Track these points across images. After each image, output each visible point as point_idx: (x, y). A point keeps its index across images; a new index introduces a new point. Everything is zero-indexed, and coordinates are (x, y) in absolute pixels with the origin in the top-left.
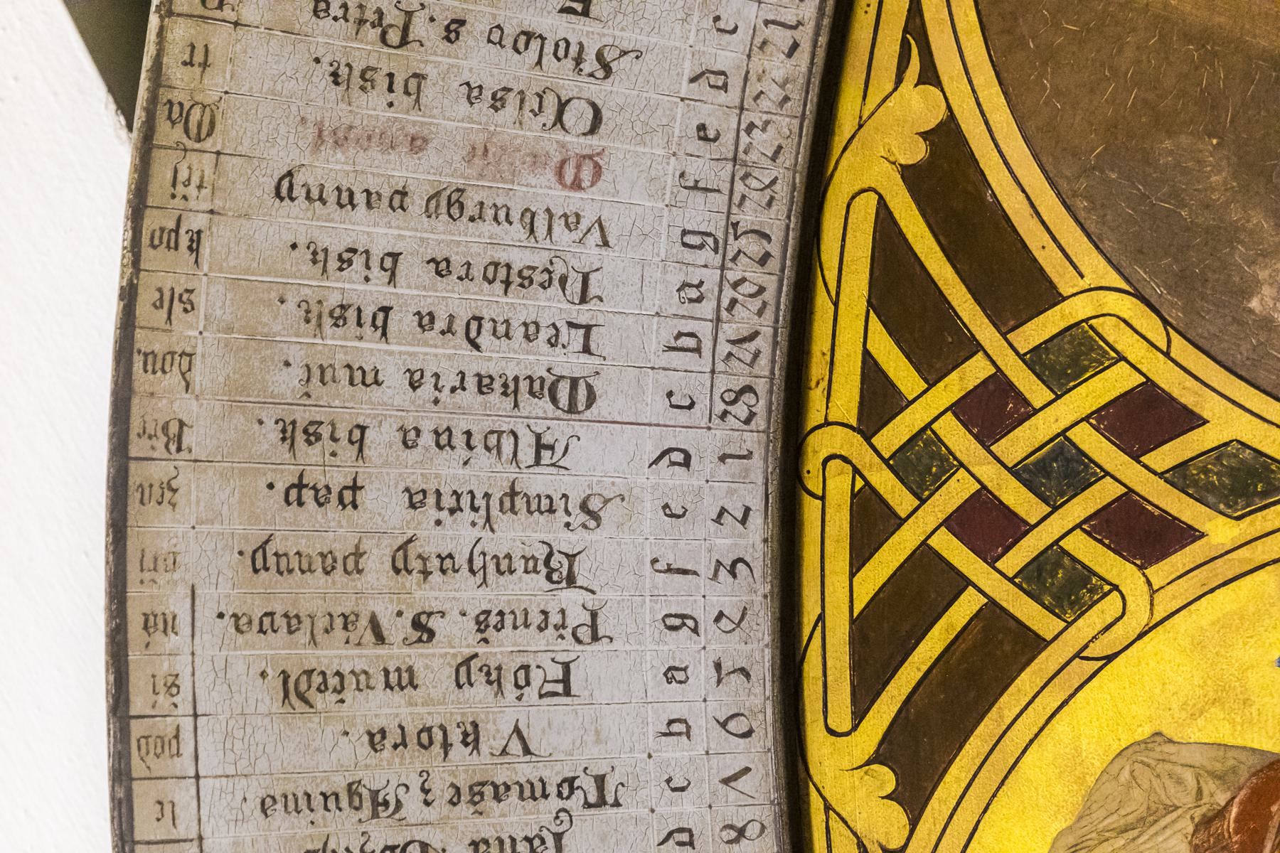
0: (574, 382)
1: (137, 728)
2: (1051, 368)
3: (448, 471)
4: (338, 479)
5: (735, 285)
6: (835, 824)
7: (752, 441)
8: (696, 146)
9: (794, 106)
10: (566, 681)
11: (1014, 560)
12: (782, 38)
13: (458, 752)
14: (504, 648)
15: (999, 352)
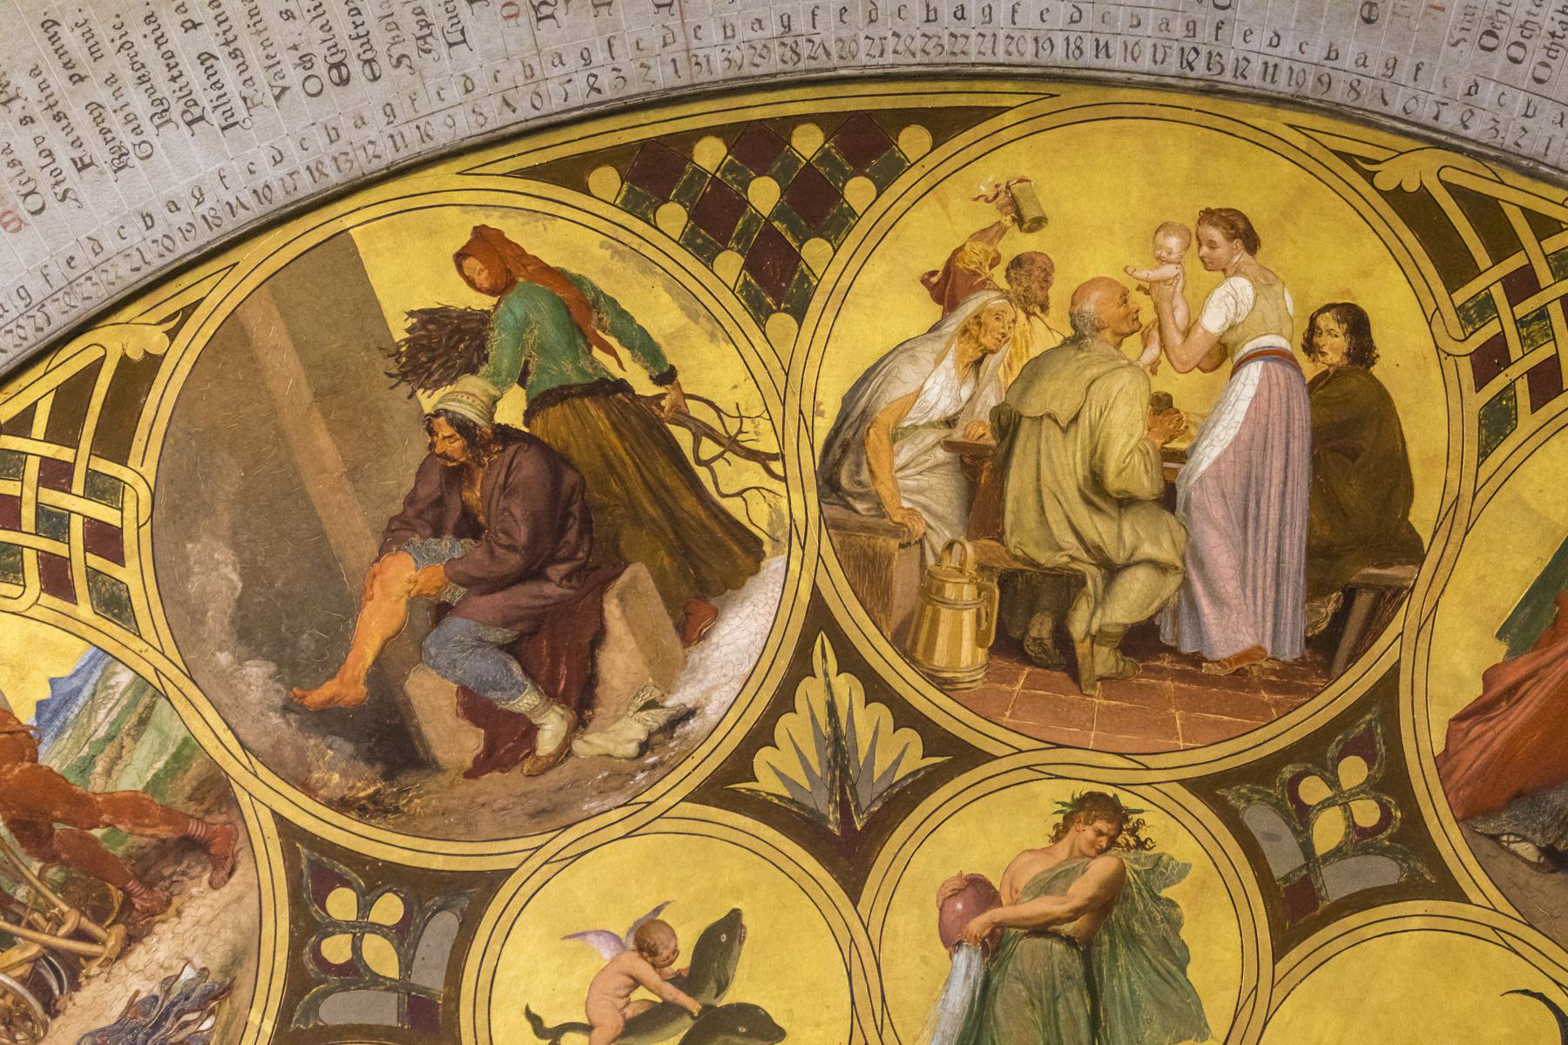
2: (93, 485)
5: (19, 326)
9: (113, 289)
12: (136, 260)
15: (82, 457)
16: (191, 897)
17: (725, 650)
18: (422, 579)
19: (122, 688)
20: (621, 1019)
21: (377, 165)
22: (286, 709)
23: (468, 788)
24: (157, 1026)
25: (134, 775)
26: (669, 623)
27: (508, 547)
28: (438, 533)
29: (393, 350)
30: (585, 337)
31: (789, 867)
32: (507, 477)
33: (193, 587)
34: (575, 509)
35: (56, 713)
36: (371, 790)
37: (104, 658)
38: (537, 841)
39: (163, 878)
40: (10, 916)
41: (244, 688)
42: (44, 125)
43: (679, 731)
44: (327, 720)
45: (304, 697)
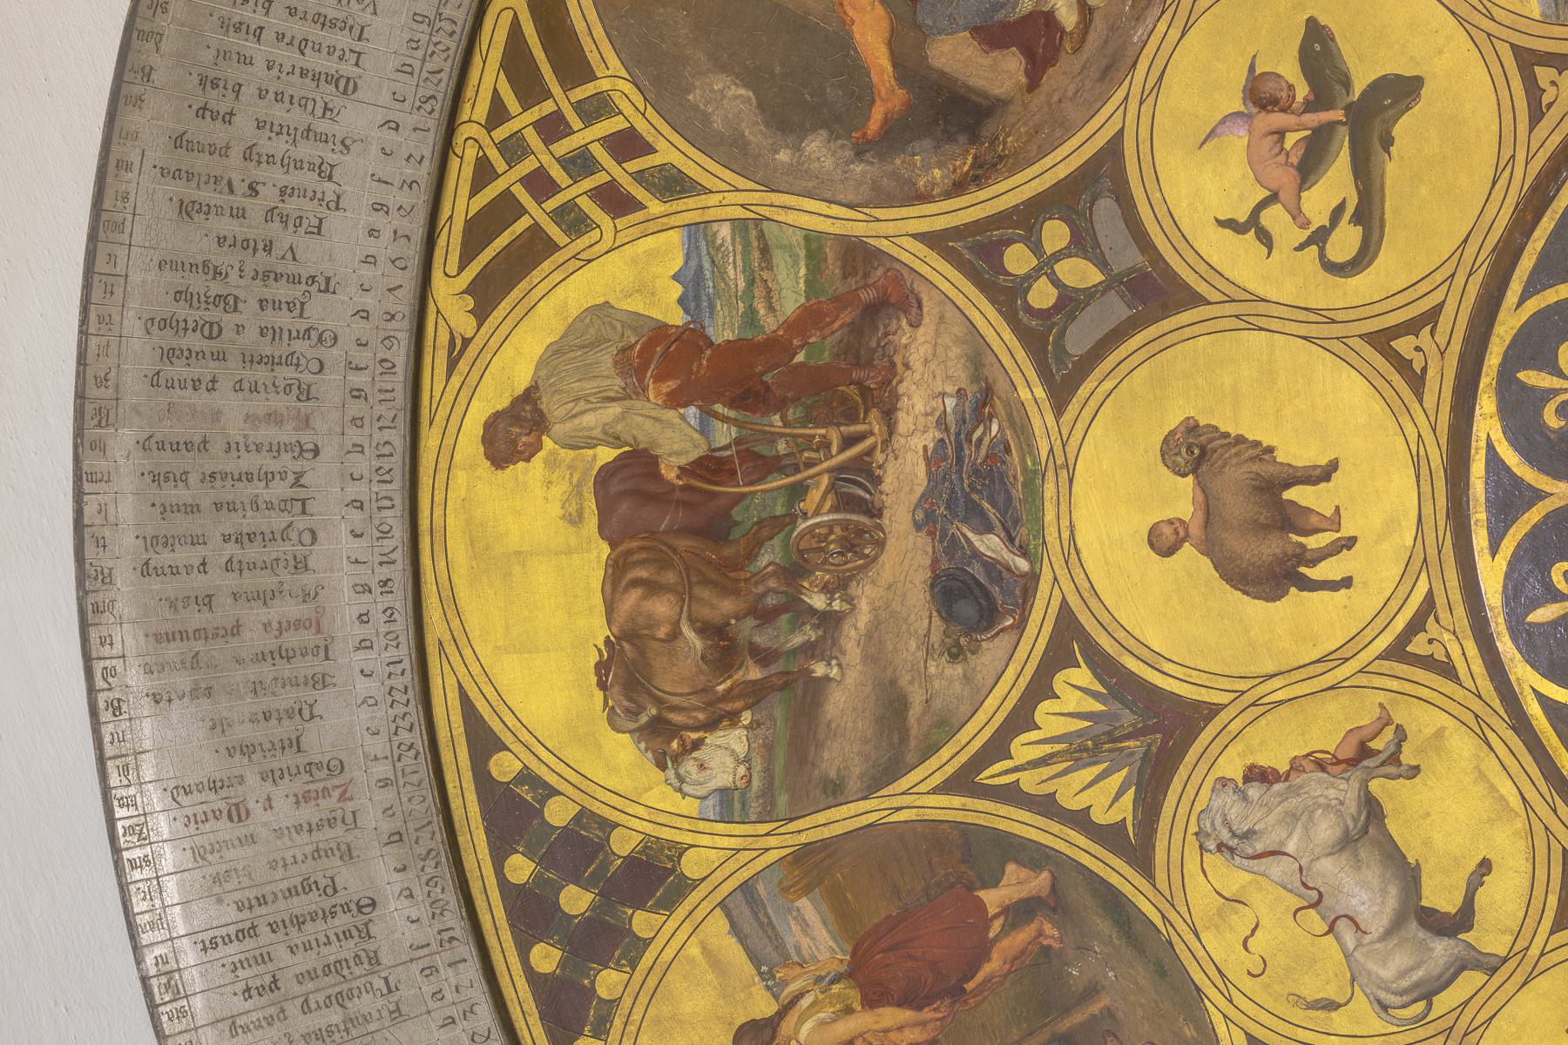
0: (348, 80)
3: (279, 113)
4: (224, 108)
6: (441, 321)
7: (431, 123)
10: (319, 228)
11: (551, 204)
13: (261, 253)
14: (291, 206)
15: (561, 100)
19: (729, 240)
22: (859, 155)
23: (1039, 98)
24: (960, 460)
25: (791, 294)
33: (718, 124)
35: (697, 298)
37: (697, 232)
38: (1121, 94)
39: (874, 351)
40: (788, 471)
41: (816, 165)
44: (895, 137)
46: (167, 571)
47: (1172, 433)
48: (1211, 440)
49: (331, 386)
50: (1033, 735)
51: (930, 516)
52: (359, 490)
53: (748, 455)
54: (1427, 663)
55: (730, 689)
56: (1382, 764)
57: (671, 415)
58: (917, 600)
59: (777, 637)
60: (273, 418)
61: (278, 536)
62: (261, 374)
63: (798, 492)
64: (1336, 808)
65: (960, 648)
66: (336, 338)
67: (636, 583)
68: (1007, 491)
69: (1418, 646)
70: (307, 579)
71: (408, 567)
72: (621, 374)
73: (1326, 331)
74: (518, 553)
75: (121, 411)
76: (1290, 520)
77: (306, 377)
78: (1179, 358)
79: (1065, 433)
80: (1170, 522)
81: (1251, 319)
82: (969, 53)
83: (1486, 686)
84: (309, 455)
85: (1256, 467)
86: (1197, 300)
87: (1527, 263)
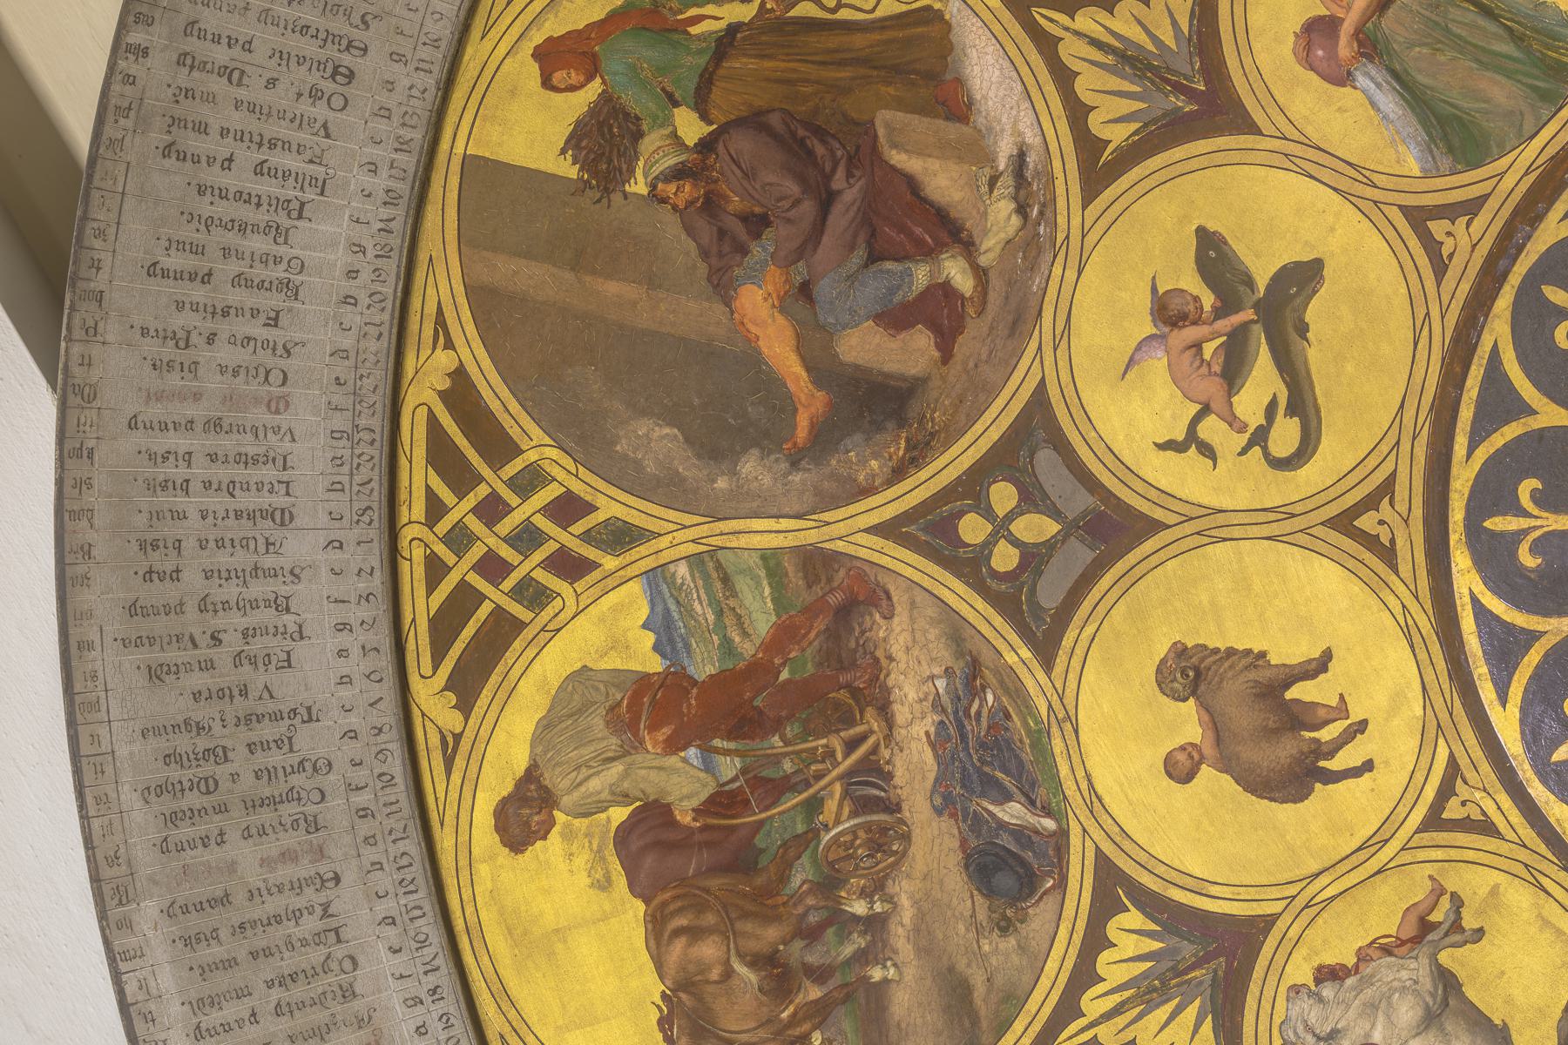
0: (283, 511)
1: (78, 699)
3: (223, 559)
4: (169, 567)
7: (373, 533)
8: (334, 388)
9: (382, 365)
10: (289, 660)
11: (508, 584)
12: (374, 331)
13: (238, 699)
14: (257, 646)
15: (493, 481)
16: (885, 640)
17: (991, 94)
18: (770, 288)
20: (1217, 379)
21: (429, 96)
22: (795, 465)
23: (956, 367)
24: (963, 737)
25: (760, 613)
26: (941, 123)
27: (793, 206)
28: (744, 251)
29: (581, 185)
30: (676, 30)
31: (1194, 164)
32: (739, 167)
33: (651, 467)
34: (801, 132)
35: (671, 641)
36: (903, 444)
37: (656, 578)
38: (1033, 345)
39: (855, 651)
40: (799, 788)
42: (224, 328)
43: (1028, 174)
44: (825, 439)
45: (795, 444)
46: (220, 1029)
47: (1163, 661)
48: (1202, 660)
49: (336, 810)
50: (1100, 988)
51: (948, 799)
52: (384, 907)
53: (757, 782)
54: (1466, 825)
55: (794, 1015)
56: (1446, 934)
57: (673, 761)
58: (956, 882)
59: (828, 951)
60: (288, 856)
61: (319, 970)
62: (266, 816)
63: (814, 806)
64: (1412, 989)
65: (1008, 920)
66: (330, 764)
67: (677, 933)
68: (1017, 757)
69: (1453, 811)
70: (358, 1005)
71: (453, 970)
72: (616, 732)
73: (1287, 526)
74: (557, 931)
75: (138, 885)
76: (1299, 718)
77: (311, 809)
78: (1151, 588)
79: (1059, 686)
80: (1183, 748)
81: (1212, 533)
82: (877, 340)
83: (1528, 834)
84: (331, 884)
85: (1253, 675)
86: (1157, 526)
87: (1466, 414)
